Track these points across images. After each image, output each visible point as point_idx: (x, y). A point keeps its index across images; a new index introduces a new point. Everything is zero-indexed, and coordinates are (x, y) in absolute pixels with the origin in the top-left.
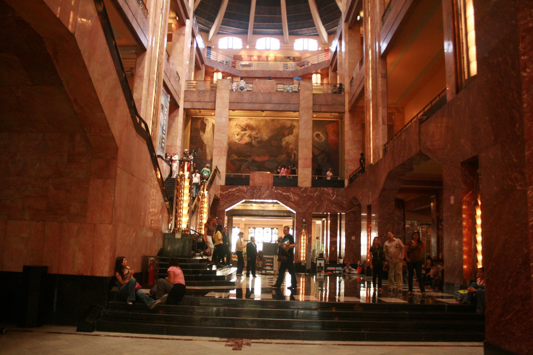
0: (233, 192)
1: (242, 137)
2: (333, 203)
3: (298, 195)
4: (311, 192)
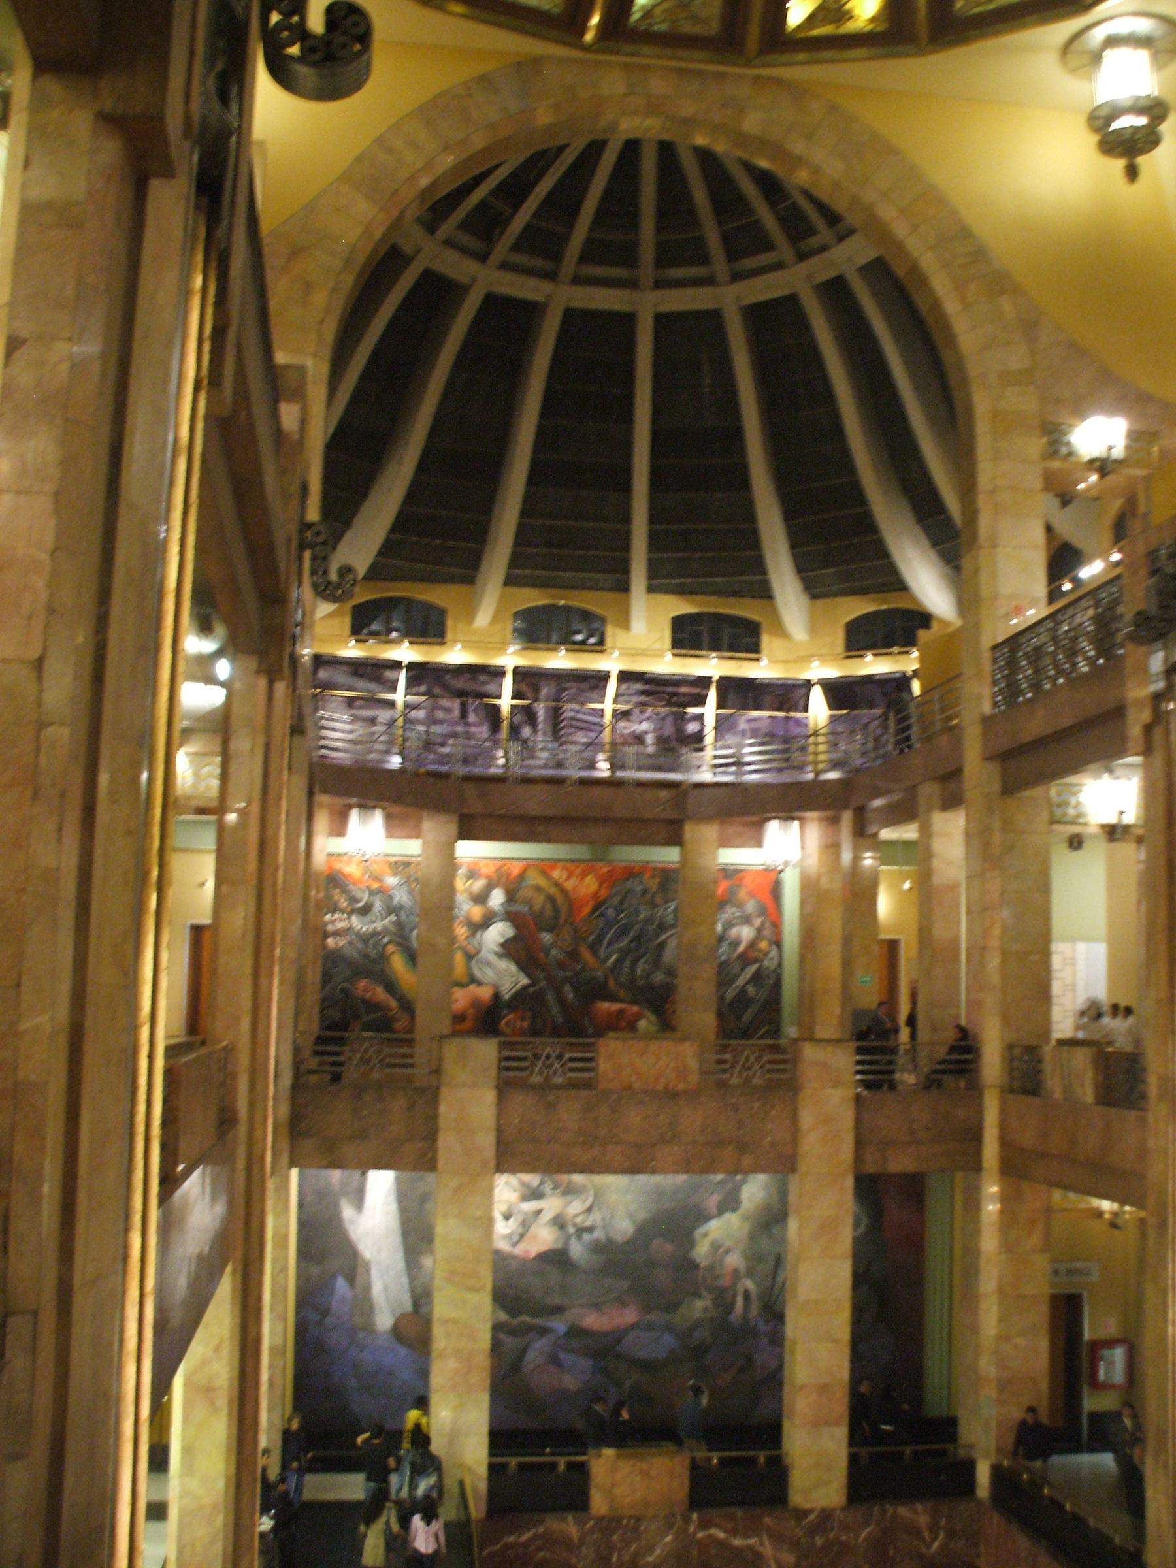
1: (526, 1225)
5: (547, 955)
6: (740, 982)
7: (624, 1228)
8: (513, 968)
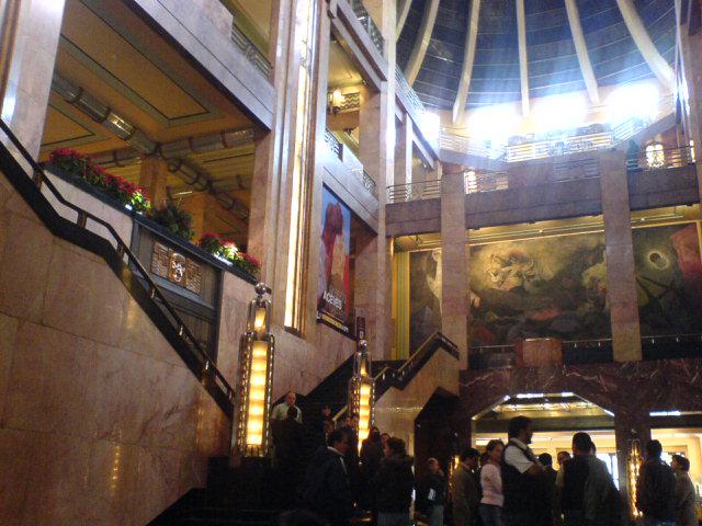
1: (504, 278)
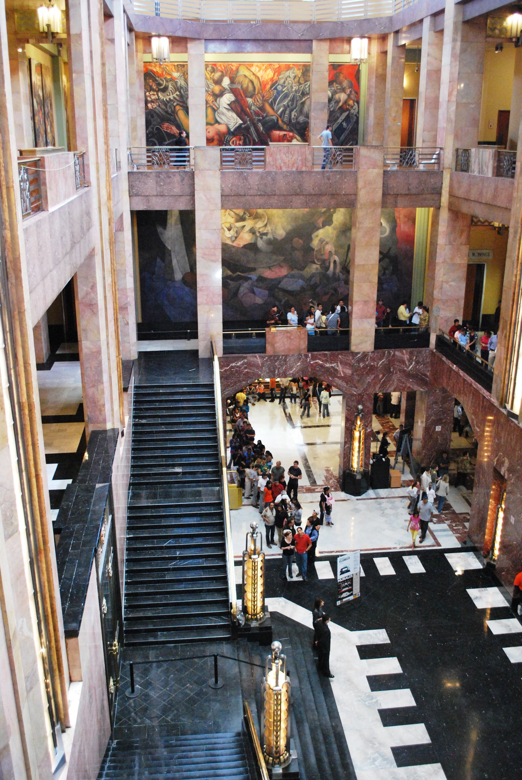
0: (237, 367)
2: (409, 375)
3: (351, 366)
4: (373, 359)
5: (250, 109)
6: (340, 121)
7: (281, 233)
8: (235, 115)
